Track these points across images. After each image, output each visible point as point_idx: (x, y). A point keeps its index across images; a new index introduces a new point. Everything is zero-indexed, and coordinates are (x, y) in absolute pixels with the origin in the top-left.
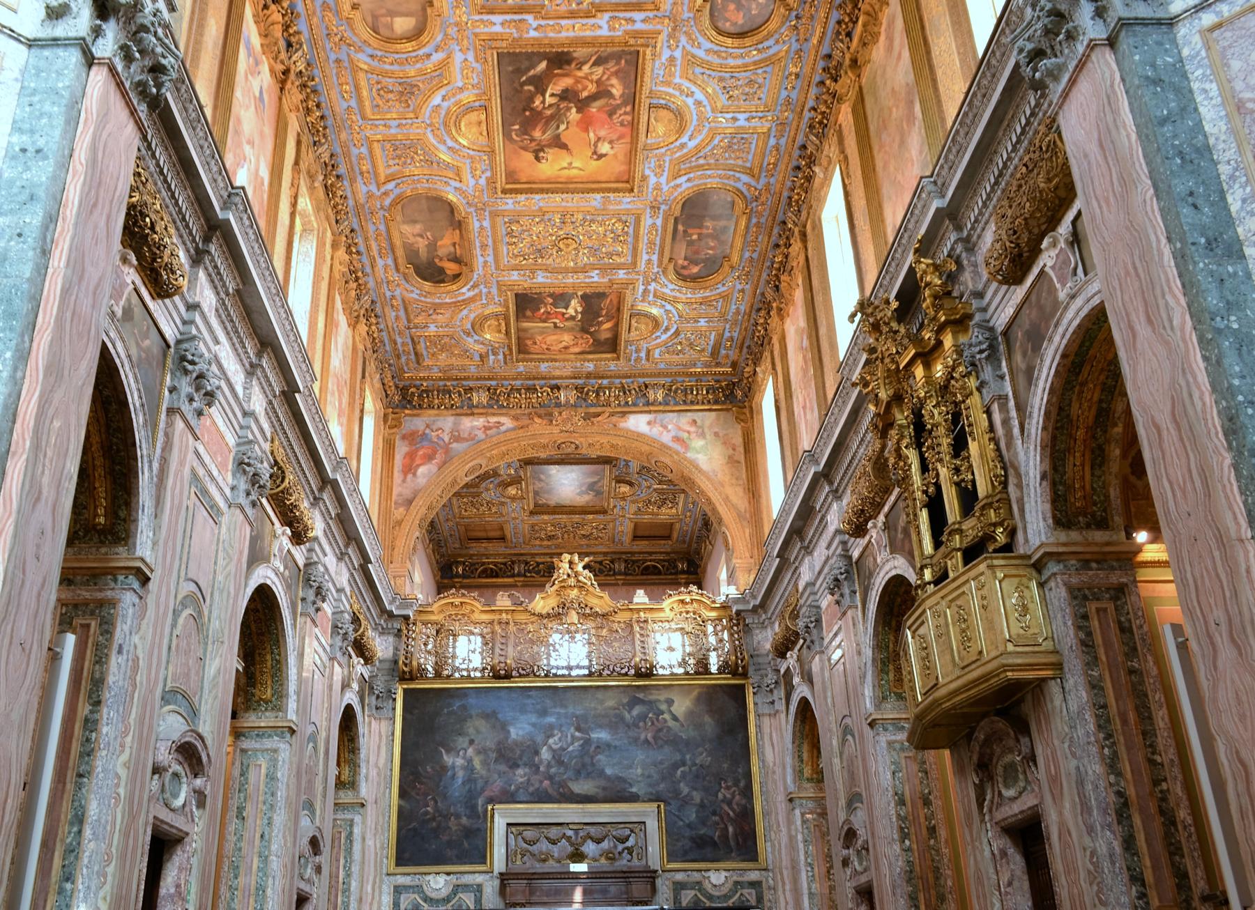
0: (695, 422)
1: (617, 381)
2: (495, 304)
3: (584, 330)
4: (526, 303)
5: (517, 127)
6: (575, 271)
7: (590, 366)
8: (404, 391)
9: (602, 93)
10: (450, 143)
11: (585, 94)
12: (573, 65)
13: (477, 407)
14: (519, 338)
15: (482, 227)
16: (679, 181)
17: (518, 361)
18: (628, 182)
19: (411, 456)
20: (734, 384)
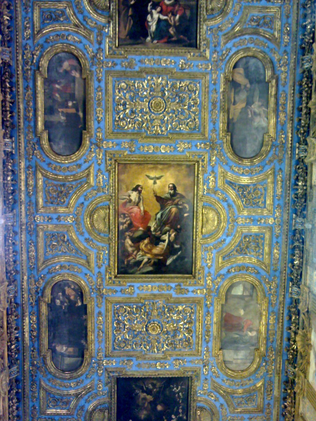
5: (186, 215)
9: (136, 241)
11: (146, 241)
12: (153, 261)
16: (87, 165)
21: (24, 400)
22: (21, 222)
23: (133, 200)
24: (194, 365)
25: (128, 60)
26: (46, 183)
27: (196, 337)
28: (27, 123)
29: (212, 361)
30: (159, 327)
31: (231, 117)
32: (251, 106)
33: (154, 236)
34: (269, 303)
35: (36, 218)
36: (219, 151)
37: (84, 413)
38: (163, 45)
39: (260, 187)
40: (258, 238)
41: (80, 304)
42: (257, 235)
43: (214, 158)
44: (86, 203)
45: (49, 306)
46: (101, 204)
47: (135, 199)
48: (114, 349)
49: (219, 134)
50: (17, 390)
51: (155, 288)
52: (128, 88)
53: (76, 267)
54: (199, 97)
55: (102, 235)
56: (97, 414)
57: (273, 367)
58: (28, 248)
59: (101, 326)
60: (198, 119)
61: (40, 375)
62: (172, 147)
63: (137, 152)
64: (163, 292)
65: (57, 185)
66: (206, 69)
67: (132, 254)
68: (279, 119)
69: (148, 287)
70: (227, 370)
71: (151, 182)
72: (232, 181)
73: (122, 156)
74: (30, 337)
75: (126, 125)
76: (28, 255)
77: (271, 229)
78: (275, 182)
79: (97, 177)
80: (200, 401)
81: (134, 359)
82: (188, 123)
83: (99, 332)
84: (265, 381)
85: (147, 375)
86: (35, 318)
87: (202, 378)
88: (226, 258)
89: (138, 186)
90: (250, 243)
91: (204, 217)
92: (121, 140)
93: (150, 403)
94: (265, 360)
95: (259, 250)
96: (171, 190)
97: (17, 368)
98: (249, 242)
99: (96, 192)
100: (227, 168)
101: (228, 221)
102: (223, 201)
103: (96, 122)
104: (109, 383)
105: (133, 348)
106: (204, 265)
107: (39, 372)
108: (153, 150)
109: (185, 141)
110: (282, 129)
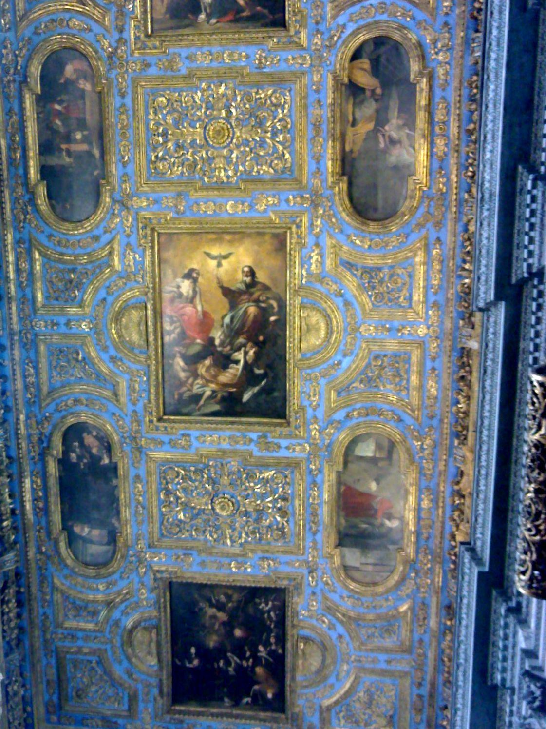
9: (193, 361)
11: (208, 362)
12: (219, 396)
21: (30, 604)
22: (11, 329)
23: (185, 294)
24: (293, 570)
25: (169, 57)
26: (47, 266)
27: (295, 523)
28: (12, 169)
29: (322, 564)
30: (233, 503)
31: (347, 148)
32: (383, 128)
33: (221, 352)
34: (420, 473)
35: (33, 324)
36: (327, 209)
37: (120, 631)
38: (227, 25)
39: (400, 271)
40: (399, 360)
42: (396, 356)
43: (319, 222)
44: (110, 299)
45: (60, 462)
46: (133, 301)
47: (188, 292)
48: (162, 535)
49: (326, 180)
50: (17, 589)
51: (224, 440)
52: (170, 105)
53: (98, 402)
54: (290, 116)
55: (136, 351)
56: (139, 635)
57: (429, 581)
58: (24, 370)
59: (141, 498)
60: (290, 153)
61: (52, 568)
62: (246, 204)
63: (188, 213)
64: (238, 447)
65: (64, 269)
66: (302, 64)
67: (186, 382)
68: (435, 150)
69: (214, 438)
70: (349, 581)
71: (213, 263)
72: (351, 261)
73: (162, 221)
74: (34, 509)
75: (169, 168)
76: (25, 381)
77: (422, 344)
78: (427, 263)
79: (125, 257)
80: (303, 628)
81: (195, 553)
82: (272, 161)
83: (137, 507)
84: (414, 602)
85: (214, 580)
86: (39, 481)
87: (307, 591)
88: (344, 394)
89: (192, 270)
90: (384, 368)
91: (303, 324)
92: (161, 194)
93: (223, 624)
94: (414, 569)
95: (401, 381)
96: (247, 276)
97: (16, 556)
98: (382, 367)
99: (124, 281)
100: (341, 238)
101: (345, 330)
102: (336, 295)
103: (120, 165)
104: (156, 588)
105: (191, 536)
106: (306, 403)
107: (50, 566)
108: (215, 211)
109: (269, 193)
110: (441, 168)
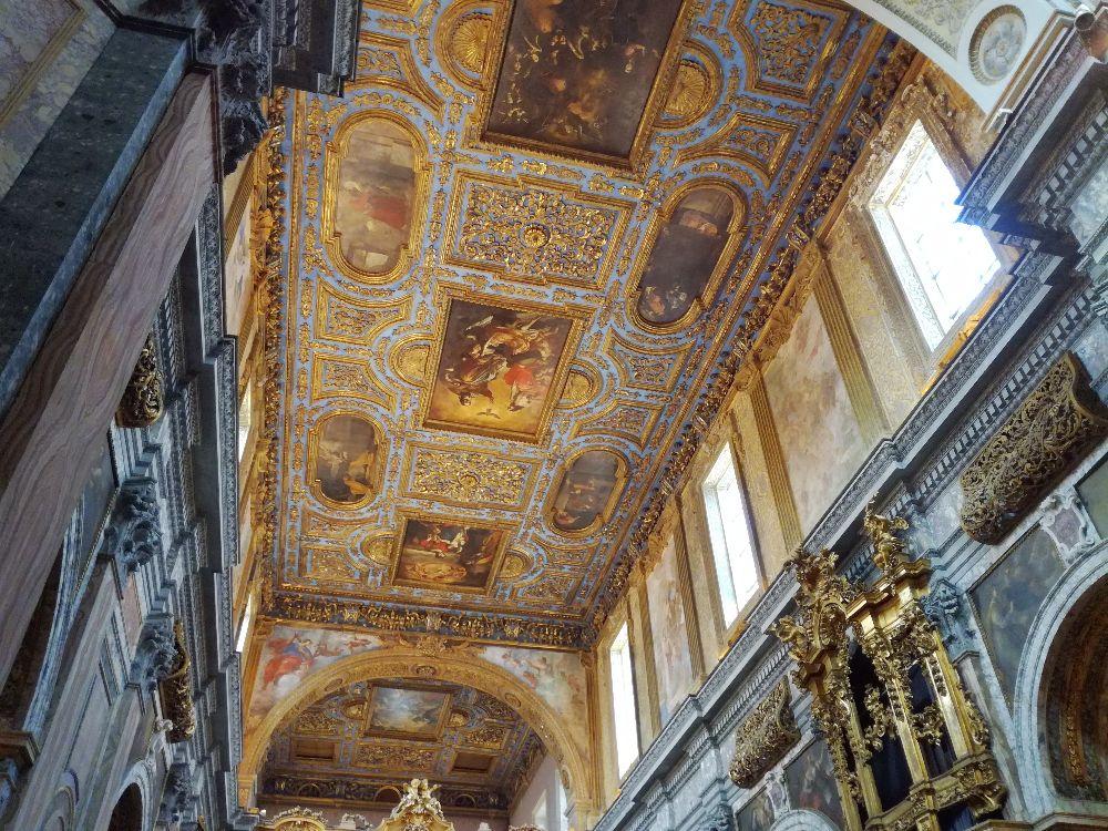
0: (544, 659)
1: (480, 614)
2: (392, 525)
3: (462, 563)
4: (416, 530)
6: (469, 507)
7: (458, 597)
8: (278, 600)
9: (533, 353)
10: (389, 374)
11: (518, 351)
13: (346, 623)
14: (400, 563)
15: (396, 455)
16: (577, 440)
17: (394, 584)
18: (534, 434)
19: (275, 664)
20: (580, 629)
41: (649, 289)
45: (699, 297)
93: (576, 99)
